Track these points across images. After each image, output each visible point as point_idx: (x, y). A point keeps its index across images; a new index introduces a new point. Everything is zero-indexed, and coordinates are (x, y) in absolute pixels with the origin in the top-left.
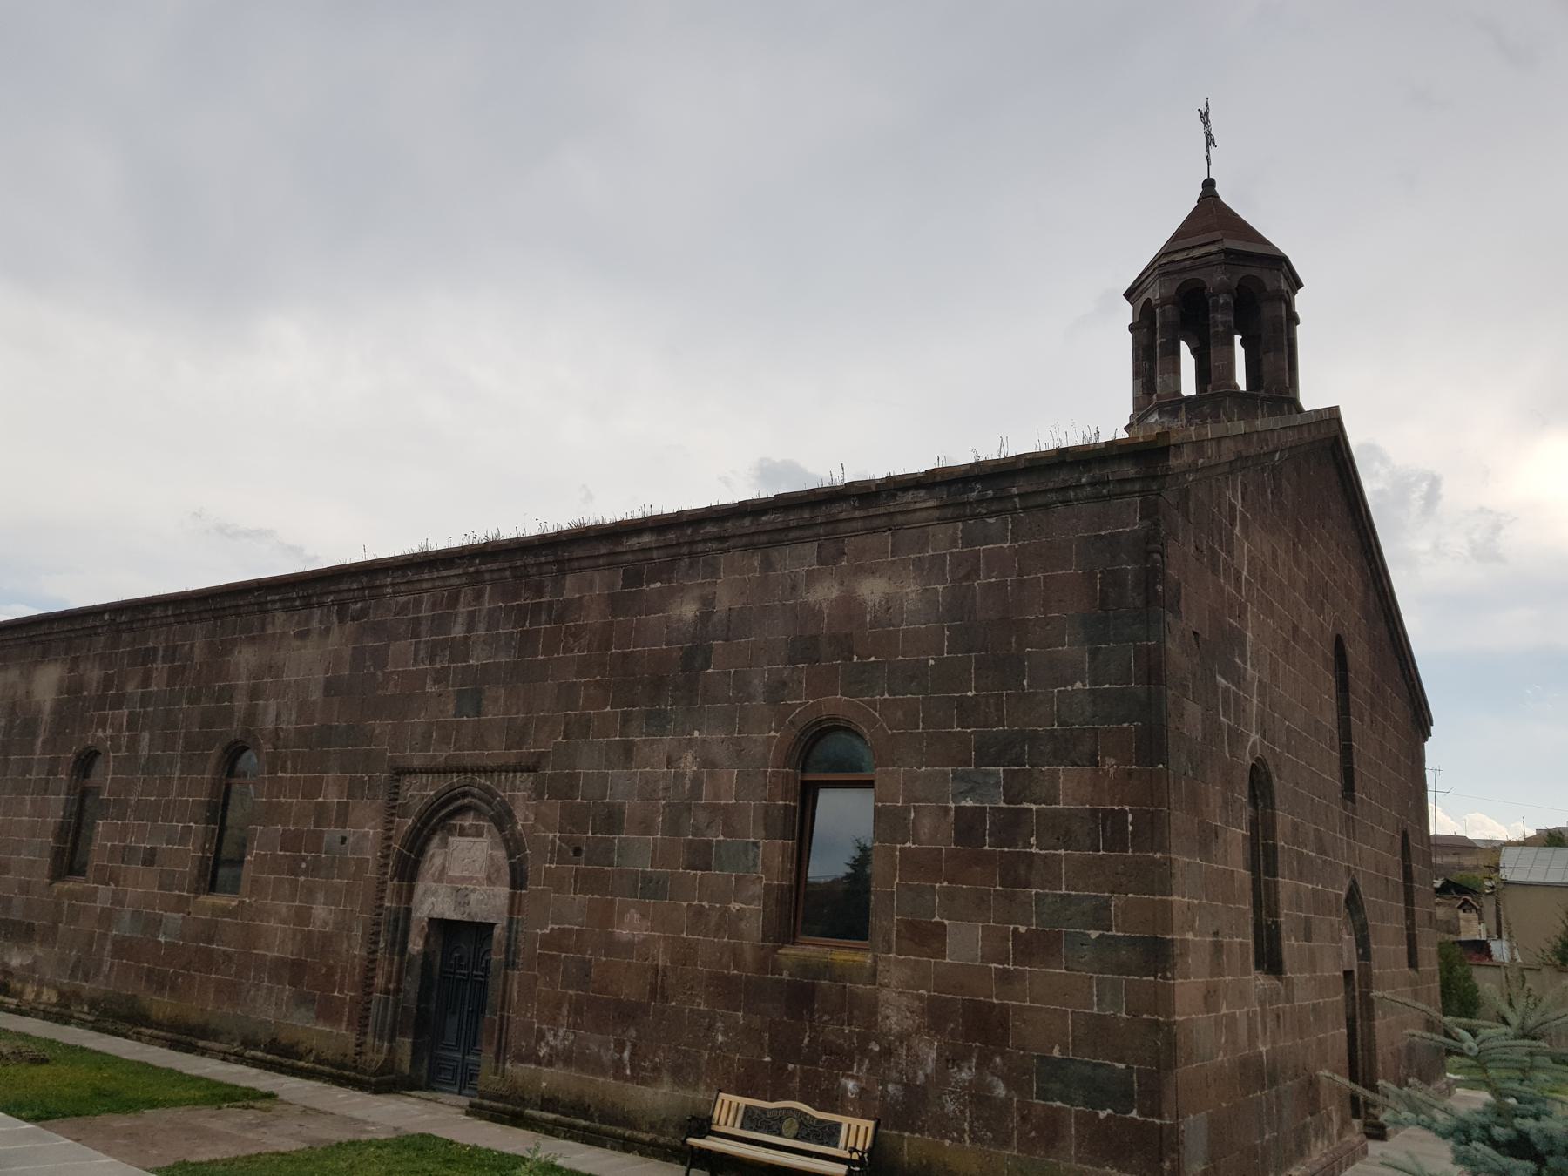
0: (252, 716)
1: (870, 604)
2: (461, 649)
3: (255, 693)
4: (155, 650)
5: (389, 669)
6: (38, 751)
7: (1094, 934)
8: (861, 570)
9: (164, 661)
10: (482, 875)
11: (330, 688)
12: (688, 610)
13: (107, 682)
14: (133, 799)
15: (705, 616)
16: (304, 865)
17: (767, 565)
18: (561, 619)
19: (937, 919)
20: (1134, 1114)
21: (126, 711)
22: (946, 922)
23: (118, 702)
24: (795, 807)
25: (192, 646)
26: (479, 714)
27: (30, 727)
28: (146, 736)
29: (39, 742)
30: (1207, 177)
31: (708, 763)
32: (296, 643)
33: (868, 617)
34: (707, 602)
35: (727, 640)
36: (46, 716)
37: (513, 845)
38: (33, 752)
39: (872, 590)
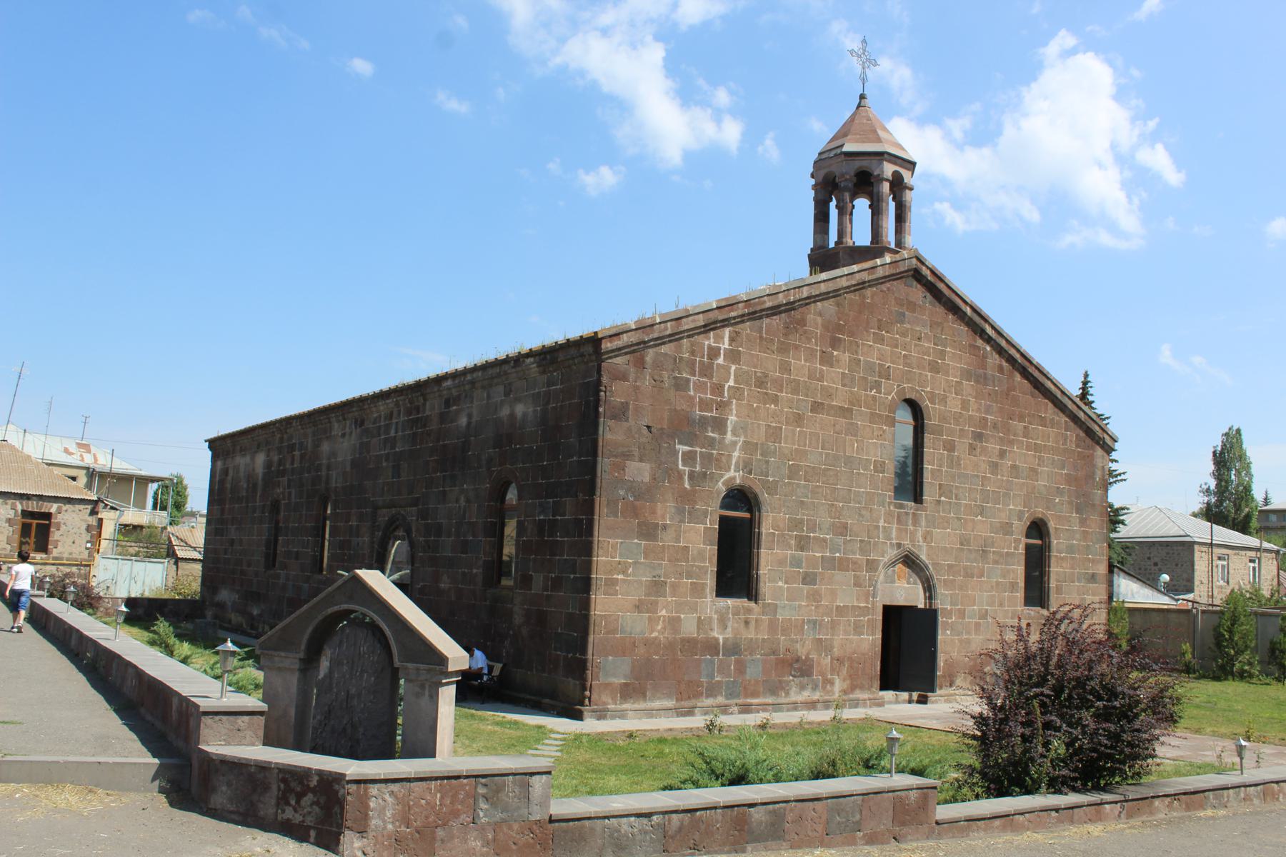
0: (328, 478)
1: (518, 417)
2: (392, 442)
3: (329, 468)
4: (295, 444)
5: (371, 454)
6: (258, 501)
7: (572, 576)
8: (518, 400)
9: (299, 451)
10: (405, 560)
11: (354, 463)
12: (463, 421)
13: (280, 462)
14: (291, 525)
15: (469, 424)
16: (346, 558)
17: (489, 397)
18: (425, 426)
19: (530, 573)
20: (577, 655)
21: (286, 478)
22: (533, 574)
23: (282, 473)
24: (496, 523)
25: (307, 443)
26: (399, 477)
27: (255, 485)
28: (293, 491)
29: (259, 494)
30: (862, 92)
31: (468, 501)
32: (342, 440)
33: (518, 425)
34: (470, 416)
35: (475, 437)
36: (260, 482)
37: (412, 545)
38: (256, 502)
39: (520, 409)
